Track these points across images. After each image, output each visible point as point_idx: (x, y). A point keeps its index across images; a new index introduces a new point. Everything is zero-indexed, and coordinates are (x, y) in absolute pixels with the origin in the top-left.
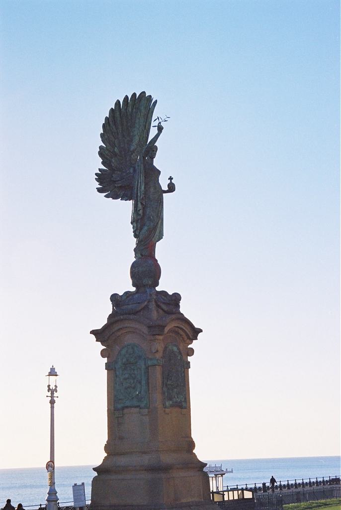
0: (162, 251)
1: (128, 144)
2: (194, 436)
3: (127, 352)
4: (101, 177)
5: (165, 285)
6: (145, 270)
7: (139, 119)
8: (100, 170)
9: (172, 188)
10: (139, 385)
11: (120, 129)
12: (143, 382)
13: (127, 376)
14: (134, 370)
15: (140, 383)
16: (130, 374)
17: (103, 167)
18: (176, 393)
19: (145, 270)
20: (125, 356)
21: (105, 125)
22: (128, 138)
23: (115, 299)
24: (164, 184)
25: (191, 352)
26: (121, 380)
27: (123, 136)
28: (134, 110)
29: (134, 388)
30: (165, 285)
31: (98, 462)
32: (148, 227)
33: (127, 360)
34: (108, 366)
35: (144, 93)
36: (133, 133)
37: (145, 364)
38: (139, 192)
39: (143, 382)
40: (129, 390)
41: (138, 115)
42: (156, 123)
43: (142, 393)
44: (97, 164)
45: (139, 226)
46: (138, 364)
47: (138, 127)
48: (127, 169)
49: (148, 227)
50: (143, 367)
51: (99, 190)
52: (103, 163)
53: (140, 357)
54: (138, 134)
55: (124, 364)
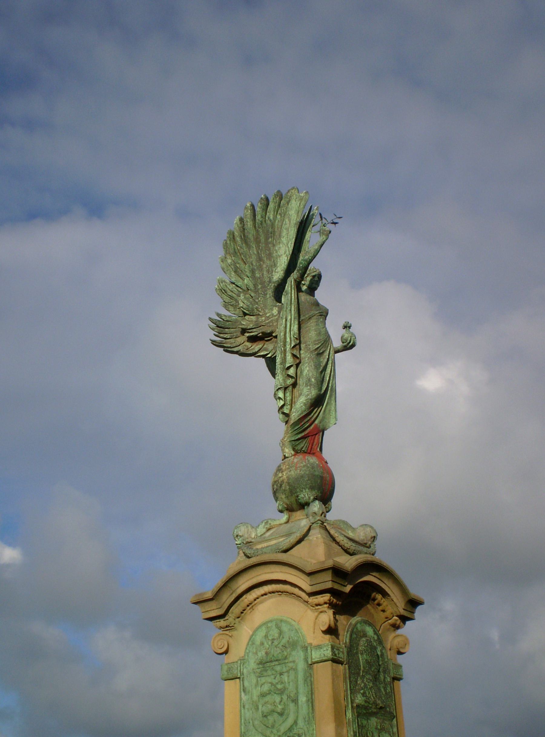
1: (268, 271)
3: (266, 636)
7: (287, 229)
8: (218, 315)
10: (292, 706)
11: (255, 249)
12: (302, 699)
13: (266, 688)
14: (281, 674)
15: (295, 701)
16: (272, 684)
17: (224, 312)
18: (376, 728)
20: (262, 644)
21: (228, 242)
22: (268, 262)
26: (255, 698)
27: (260, 259)
28: (279, 217)
29: (281, 714)
33: (267, 653)
36: (277, 252)
37: (306, 660)
38: (288, 335)
39: (302, 699)
40: (271, 719)
41: (285, 224)
43: (301, 723)
45: (289, 398)
46: (291, 659)
47: (285, 242)
48: (267, 311)
50: (301, 666)
52: (226, 305)
53: (293, 645)
54: (285, 253)
55: (261, 663)
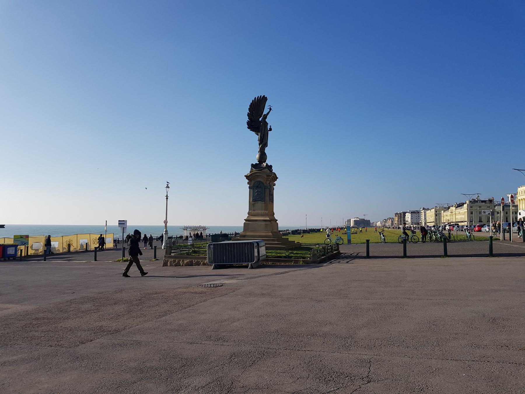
0: (267, 150)
2: (275, 211)
4: (248, 123)
5: (269, 162)
6: (263, 157)
9: (271, 130)
19: (263, 157)
23: (253, 166)
24: (269, 127)
25: (274, 185)
30: (269, 162)
31: (246, 218)
32: (263, 143)
34: (250, 188)
35: (264, 96)
42: (269, 107)
44: (247, 119)
49: (263, 143)
51: (248, 128)
